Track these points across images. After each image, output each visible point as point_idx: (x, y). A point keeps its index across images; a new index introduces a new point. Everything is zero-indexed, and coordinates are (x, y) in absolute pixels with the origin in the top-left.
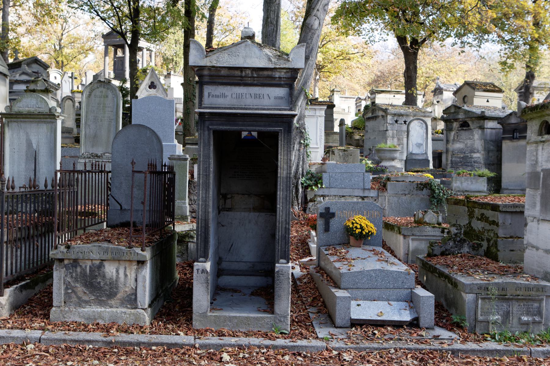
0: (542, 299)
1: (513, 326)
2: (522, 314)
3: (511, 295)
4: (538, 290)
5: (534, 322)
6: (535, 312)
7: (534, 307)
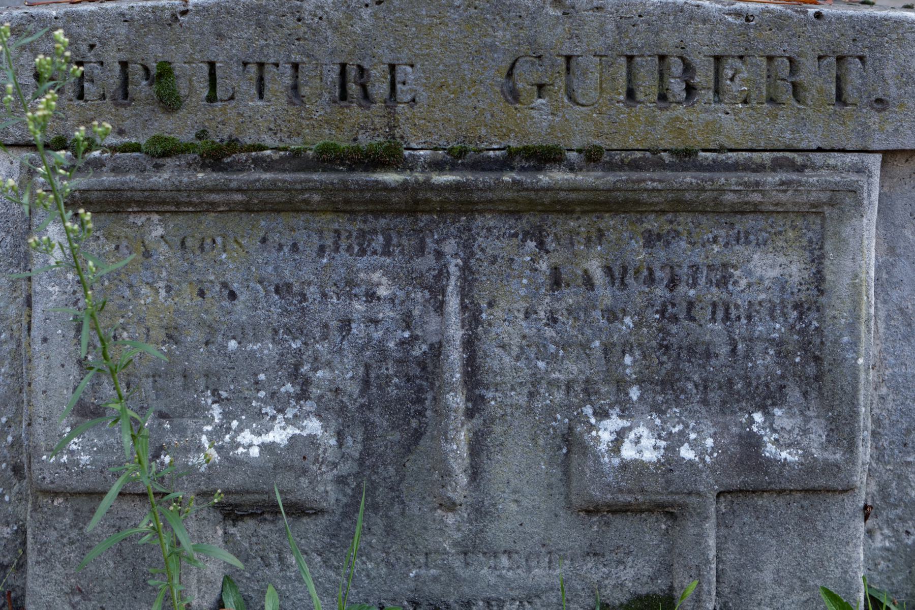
0: (842, 200)
1: (498, 532)
2: (604, 391)
3: (456, 158)
4: (785, 84)
5: (749, 482)
6: (764, 362)
7: (741, 293)
